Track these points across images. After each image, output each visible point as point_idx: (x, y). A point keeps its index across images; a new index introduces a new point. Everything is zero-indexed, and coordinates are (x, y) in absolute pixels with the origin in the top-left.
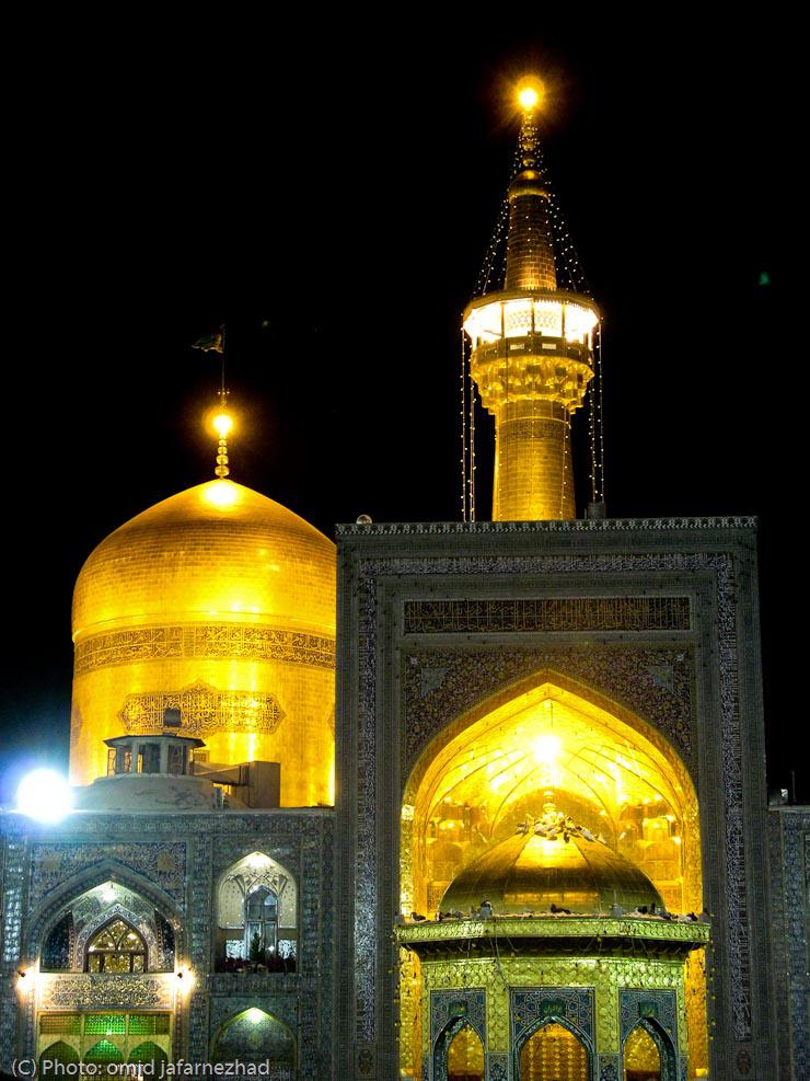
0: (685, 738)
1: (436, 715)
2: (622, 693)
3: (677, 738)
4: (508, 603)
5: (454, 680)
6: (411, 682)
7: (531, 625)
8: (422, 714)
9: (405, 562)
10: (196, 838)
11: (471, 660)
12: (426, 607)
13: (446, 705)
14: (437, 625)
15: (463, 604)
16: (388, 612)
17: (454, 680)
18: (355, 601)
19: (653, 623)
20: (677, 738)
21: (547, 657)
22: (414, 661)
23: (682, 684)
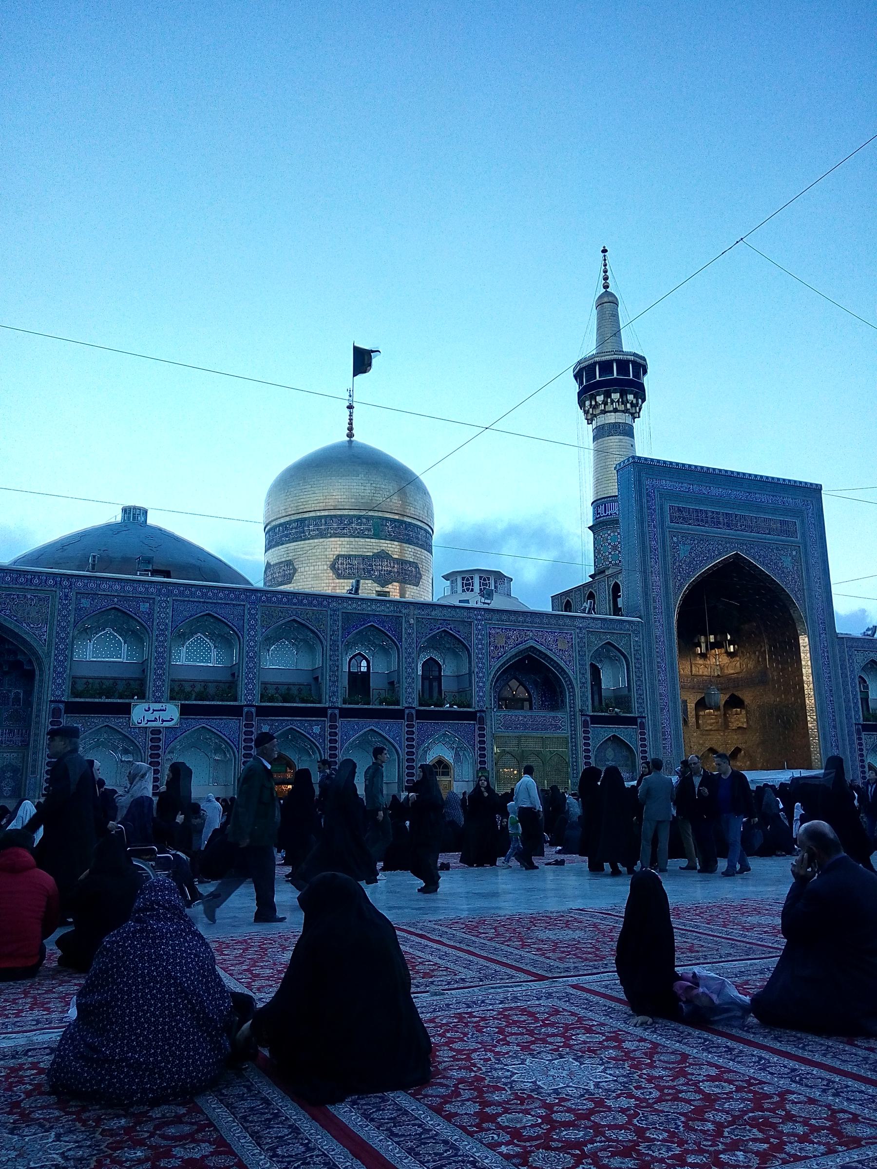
12: (679, 510)
16: (662, 509)
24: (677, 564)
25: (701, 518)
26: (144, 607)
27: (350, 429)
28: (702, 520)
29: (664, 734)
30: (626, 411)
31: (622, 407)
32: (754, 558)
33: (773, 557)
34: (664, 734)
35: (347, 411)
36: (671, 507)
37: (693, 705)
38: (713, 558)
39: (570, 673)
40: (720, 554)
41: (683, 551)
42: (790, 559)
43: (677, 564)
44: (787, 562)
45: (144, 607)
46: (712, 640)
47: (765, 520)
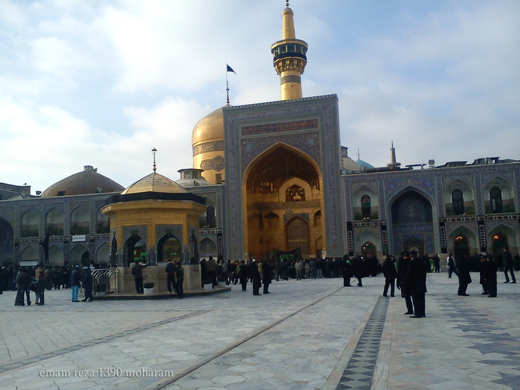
7: (275, 130)
14: (250, 133)
16: (237, 129)
18: (228, 128)
22: (244, 143)
25: (260, 129)
26: (37, 207)
27: (228, 100)
29: (233, 235)
30: (294, 69)
31: (291, 67)
32: (290, 143)
33: (302, 141)
34: (233, 235)
35: (226, 91)
37: (313, 216)
38: (264, 148)
40: (269, 145)
41: (249, 147)
42: (312, 140)
44: (311, 142)
45: (37, 207)
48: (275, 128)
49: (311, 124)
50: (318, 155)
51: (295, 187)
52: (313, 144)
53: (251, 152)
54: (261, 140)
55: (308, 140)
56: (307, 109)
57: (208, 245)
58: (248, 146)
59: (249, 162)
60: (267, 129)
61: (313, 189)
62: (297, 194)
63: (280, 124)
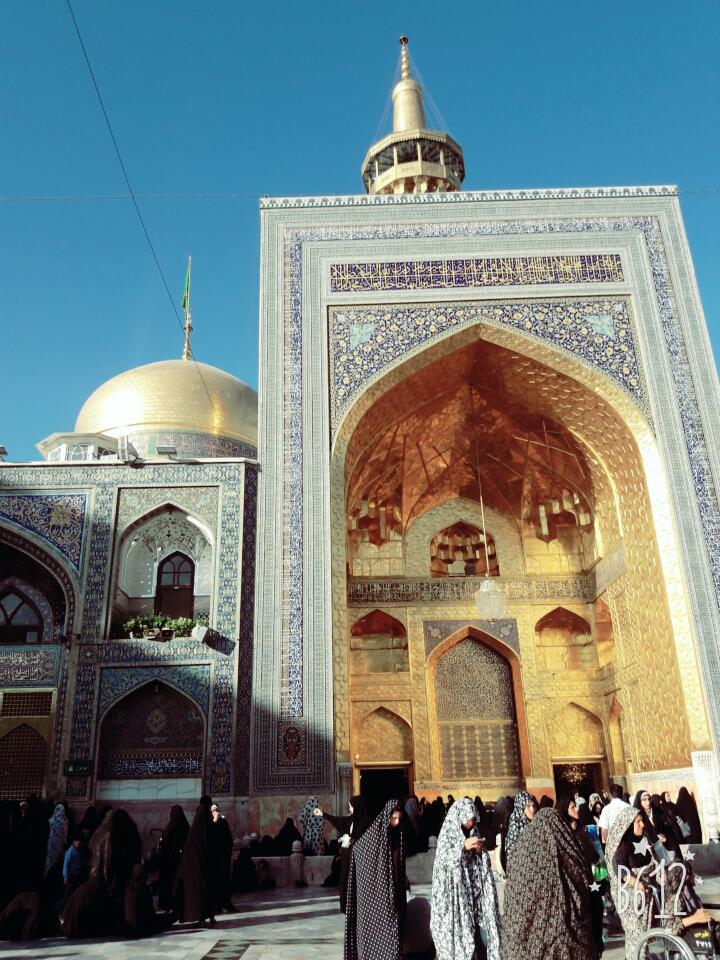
0: (634, 382)
1: (365, 367)
2: (562, 341)
3: (625, 382)
4: (435, 264)
5: (384, 334)
6: (339, 337)
7: (461, 281)
8: (352, 366)
9: (330, 230)
10: (99, 490)
11: (400, 315)
12: (352, 269)
13: (376, 357)
14: (365, 284)
15: (391, 266)
16: (314, 271)
17: (384, 334)
19: (585, 276)
20: (625, 382)
21: (479, 311)
22: (341, 318)
23: (624, 332)
24: (344, 358)
25: (401, 275)
28: (401, 279)
32: (520, 326)
36: (336, 269)
37: (531, 629)
39: (69, 567)
40: (441, 329)
41: (360, 335)
42: (607, 319)
43: (344, 358)
44: (602, 326)
46: (556, 509)
47: (547, 260)
48: (461, 273)
49: (595, 268)
50: (635, 370)
51: (462, 529)
52: (611, 334)
53: (368, 349)
54: (408, 311)
55: (590, 319)
56: (580, 225)
57: (157, 719)
58: (355, 329)
59: (358, 383)
60: (431, 274)
61: (526, 542)
62: (459, 556)
63: (478, 262)
